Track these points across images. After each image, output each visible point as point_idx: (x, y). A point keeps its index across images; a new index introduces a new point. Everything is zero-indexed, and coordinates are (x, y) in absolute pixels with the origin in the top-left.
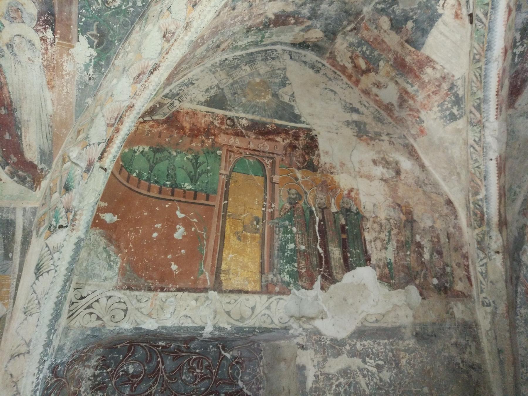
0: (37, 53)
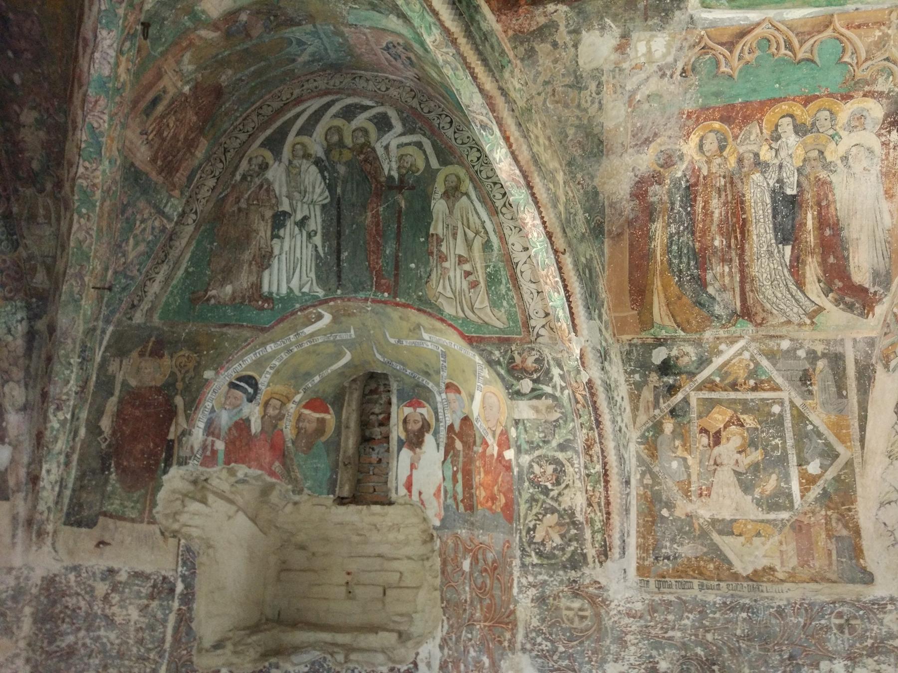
0: (875, 161)
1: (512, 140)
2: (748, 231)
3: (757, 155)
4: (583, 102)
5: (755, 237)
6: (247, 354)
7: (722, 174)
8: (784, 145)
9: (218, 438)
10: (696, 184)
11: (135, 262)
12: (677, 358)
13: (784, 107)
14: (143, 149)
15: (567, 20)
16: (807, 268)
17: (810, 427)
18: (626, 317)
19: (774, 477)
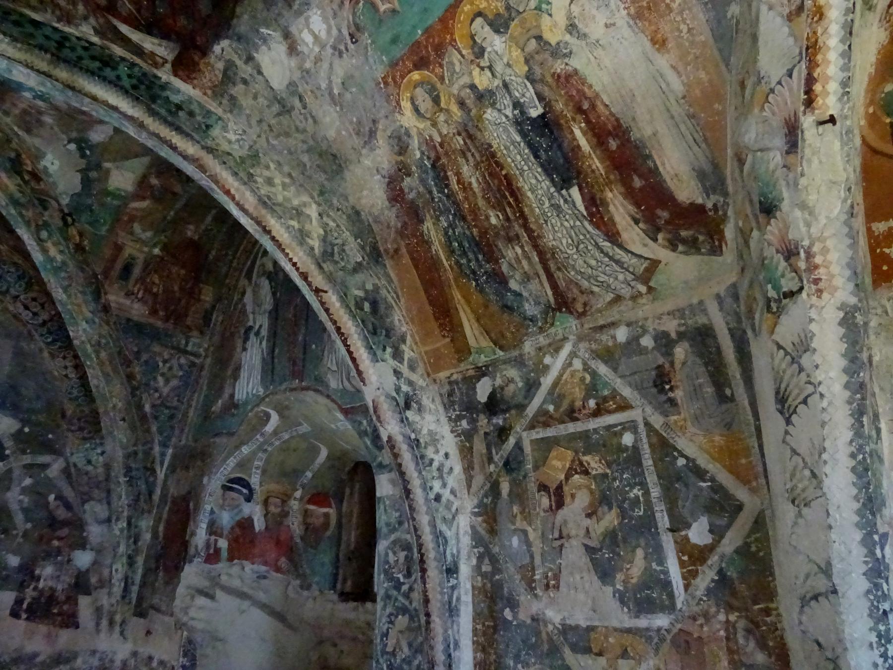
1: (233, 191)
2: (518, 188)
3: (473, 87)
4: (298, 123)
5: (529, 194)
6: (227, 458)
7: (455, 131)
8: (493, 56)
9: (221, 536)
10: (438, 158)
11: (172, 395)
12: (502, 388)
13: (466, 9)
14: (136, 306)
15: (236, 53)
16: (612, 208)
17: (681, 462)
18: (438, 349)
19: (640, 553)
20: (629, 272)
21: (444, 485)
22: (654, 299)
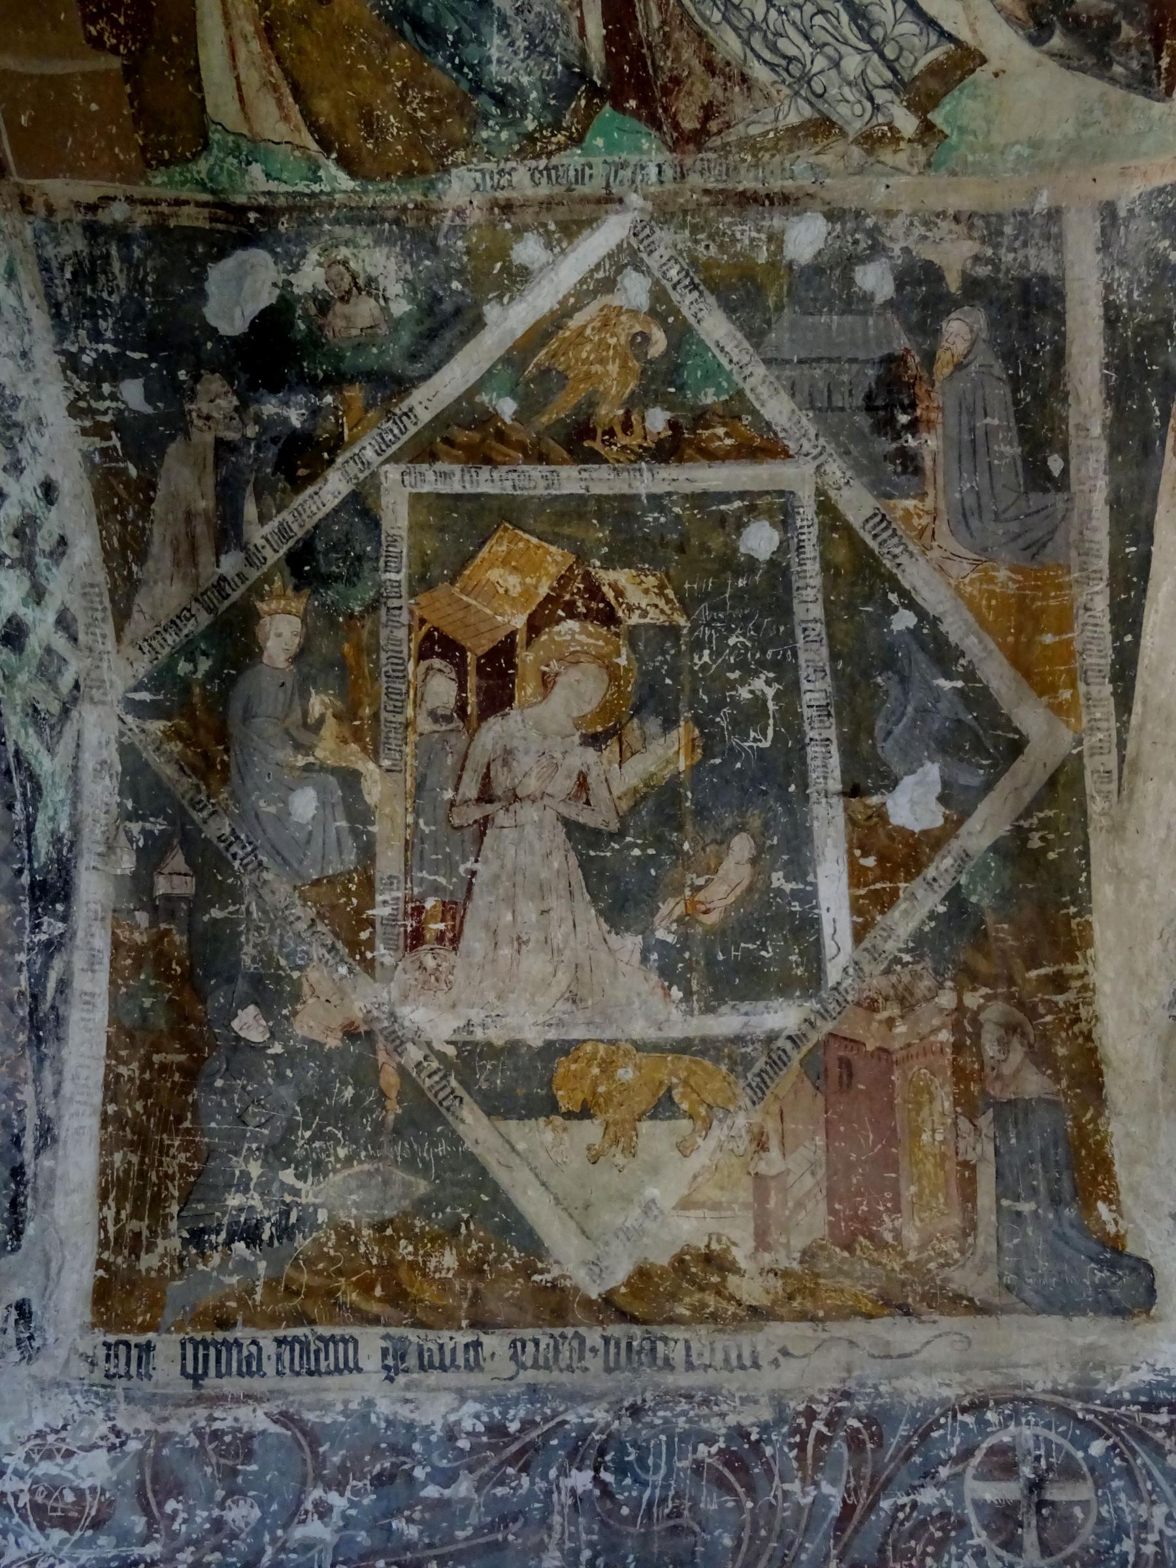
12: (324, 306)
17: (904, 620)
18: (60, 83)
19: (742, 846)
20: (882, 56)
21: (37, 594)
22: (929, 165)
